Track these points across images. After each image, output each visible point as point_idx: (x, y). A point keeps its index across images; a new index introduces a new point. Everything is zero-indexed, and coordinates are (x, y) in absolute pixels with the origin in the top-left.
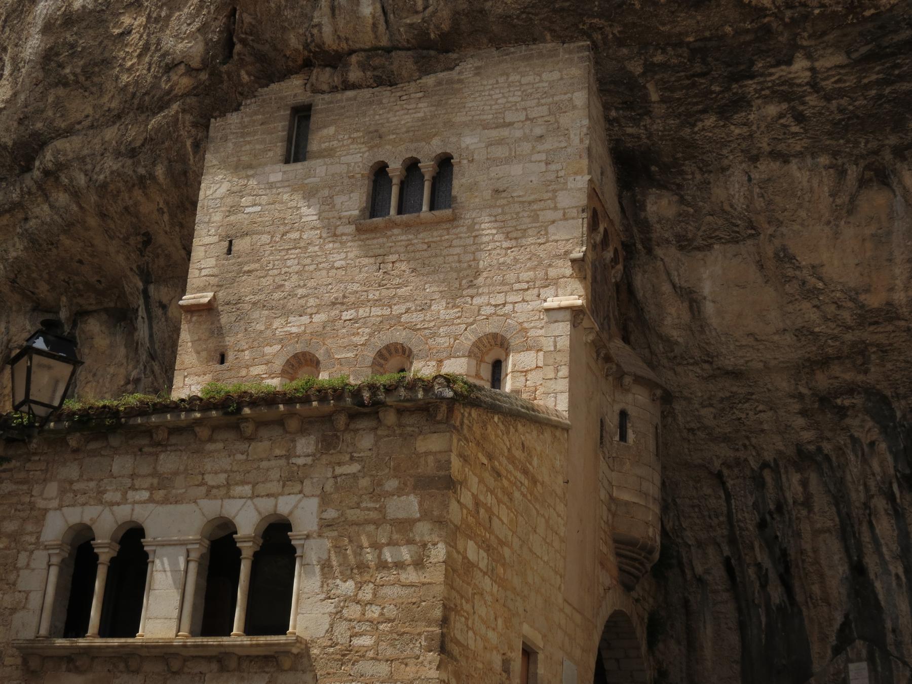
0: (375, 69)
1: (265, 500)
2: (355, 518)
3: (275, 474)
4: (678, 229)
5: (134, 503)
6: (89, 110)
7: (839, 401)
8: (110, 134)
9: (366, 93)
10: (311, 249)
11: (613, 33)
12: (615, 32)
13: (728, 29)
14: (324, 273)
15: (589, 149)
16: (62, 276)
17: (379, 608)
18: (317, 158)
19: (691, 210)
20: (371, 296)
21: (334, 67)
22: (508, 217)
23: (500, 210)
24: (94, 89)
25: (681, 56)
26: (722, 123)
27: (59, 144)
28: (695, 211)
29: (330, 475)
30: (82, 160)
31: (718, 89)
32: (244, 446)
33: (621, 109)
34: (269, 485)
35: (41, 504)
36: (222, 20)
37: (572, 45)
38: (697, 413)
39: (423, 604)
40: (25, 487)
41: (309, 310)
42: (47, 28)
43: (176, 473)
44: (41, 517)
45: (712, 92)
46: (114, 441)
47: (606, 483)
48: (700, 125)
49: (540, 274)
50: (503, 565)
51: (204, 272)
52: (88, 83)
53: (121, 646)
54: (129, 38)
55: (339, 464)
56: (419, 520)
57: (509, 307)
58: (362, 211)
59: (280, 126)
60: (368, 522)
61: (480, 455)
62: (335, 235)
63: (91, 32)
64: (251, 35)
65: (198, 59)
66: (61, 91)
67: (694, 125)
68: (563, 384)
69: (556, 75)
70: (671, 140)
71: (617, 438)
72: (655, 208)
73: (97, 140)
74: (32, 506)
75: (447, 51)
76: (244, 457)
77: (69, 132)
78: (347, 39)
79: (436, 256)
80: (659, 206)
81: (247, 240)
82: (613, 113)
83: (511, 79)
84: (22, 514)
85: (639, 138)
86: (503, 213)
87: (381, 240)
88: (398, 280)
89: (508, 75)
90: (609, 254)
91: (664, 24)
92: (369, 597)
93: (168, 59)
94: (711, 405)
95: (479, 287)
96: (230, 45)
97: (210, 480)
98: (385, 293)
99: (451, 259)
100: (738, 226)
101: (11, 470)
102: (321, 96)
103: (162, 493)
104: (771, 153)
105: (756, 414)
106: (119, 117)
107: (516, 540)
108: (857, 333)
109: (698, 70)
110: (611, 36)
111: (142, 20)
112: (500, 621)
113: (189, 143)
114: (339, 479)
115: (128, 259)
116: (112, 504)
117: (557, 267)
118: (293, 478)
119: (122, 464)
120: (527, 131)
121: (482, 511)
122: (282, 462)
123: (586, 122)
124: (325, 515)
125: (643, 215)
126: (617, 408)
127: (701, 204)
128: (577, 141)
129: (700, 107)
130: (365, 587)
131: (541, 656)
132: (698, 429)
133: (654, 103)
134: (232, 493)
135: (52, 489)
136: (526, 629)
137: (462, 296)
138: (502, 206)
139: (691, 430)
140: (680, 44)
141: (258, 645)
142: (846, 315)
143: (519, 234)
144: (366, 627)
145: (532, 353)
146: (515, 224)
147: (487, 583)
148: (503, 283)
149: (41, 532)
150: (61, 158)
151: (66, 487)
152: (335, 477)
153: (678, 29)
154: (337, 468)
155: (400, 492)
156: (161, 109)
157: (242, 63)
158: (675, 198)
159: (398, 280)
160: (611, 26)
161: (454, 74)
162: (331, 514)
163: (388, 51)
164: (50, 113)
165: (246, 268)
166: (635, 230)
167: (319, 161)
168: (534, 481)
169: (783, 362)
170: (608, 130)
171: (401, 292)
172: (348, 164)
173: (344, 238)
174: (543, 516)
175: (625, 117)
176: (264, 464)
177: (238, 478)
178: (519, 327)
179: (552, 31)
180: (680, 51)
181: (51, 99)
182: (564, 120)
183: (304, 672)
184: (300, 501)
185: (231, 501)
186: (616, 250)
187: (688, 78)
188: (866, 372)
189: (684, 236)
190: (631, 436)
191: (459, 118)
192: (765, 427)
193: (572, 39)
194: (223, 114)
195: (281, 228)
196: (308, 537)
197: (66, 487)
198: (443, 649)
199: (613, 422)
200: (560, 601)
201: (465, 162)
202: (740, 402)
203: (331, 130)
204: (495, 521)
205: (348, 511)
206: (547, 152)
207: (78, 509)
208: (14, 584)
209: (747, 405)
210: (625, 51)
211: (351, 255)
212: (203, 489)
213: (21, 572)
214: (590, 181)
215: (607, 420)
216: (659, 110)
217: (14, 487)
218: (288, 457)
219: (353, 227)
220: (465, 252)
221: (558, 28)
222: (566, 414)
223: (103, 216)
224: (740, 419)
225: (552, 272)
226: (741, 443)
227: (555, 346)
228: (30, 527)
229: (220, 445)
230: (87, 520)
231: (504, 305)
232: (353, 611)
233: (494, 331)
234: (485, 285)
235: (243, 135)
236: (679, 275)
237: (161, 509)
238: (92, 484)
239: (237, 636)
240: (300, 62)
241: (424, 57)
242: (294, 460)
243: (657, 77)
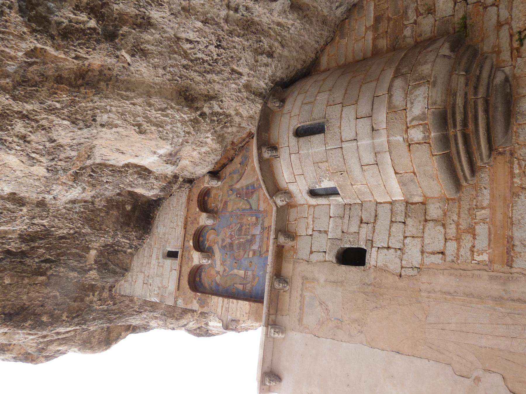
7: (92, 23)
11: (93, 295)
12: (91, 297)
25: (56, 271)
26: (53, 229)
31: (42, 250)
33: (122, 251)
38: (252, 72)
45: (47, 249)
48: (72, 231)
67: (76, 232)
70: (101, 229)
82: (129, 251)
91: (55, 297)
94: (233, 71)
100: (90, 175)
104: (23, 205)
105: (198, 42)
108: (16, 107)
110: (96, 294)
127: (109, 188)
132: (262, 54)
133: (96, 249)
139: (270, 55)
142: (19, 127)
153: (46, 291)
169: (128, 98)
188: (32, 53)
189: (140, 177)
192: (199, 24)
202: (204, 61)
209: (200, 55)
216: (96, 245)
224: (217, 47)
226: (239, 15)
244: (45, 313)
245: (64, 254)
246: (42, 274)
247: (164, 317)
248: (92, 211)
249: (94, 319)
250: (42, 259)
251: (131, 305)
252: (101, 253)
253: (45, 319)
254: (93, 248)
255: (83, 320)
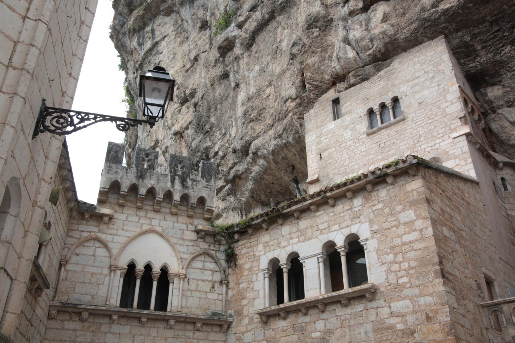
0: (359, 76)
1: (345, 229)
2: (386, 226)
3: (347, 218)
4: (506, 99)
5: (293, 244)
6: (262, 127)
8: (271, 132)
9: (358, 86)
10: (351, 148)
13: (505, 7)
14: (358, 155)
15: (455, 75)
16: (268, 191)
17: (407, 263)
18: (346, 115)
19: (509, 89)
20: (379, 158)
21: (344, 81)
22: (427, 111)
23: (423, 110)
24: (262, 119)
25: (486, 26)
27: (255, 142)
28: (511, 89)
29: (371, 211)
30: (264, 144)
31: (507, 34)
32: (331, 210)
33: (466, 58)
34: (346, 223)
35: (257, 254)
36: (300, 78)
37: (436, 39)
39: (428, 257)
40: (251, 249)
41: (356, 170)
42: (243, 104)
43: (307, 228)
44: (258, 259)
46: (280, 221)
47: (504, 209)
48: (503, 52)
49: (448, 128)
50: (464, 239)
51: (313, 168)
52: (260, 118)
53: (298, 305)
54: (270, 97)
55: (374, 206)
56: (416, 220)
57: (437, 146)
58: (368, 128)
59: (329, 107)
60: (393, 227)
61: (439, 190)
62: (359, 140)
63: (257, 100)
64: (311, 79)
65: (294, 95)
66: (252, 124)
67: (501, 53)
68: (471, 166)
69: (433, 52)
70: (492, 63)
71: (503, 189)
72: (492, 94)
73: (267, 136)
74: (254, 256)
75: (386, 60)
76: (333, 214)
77: (258, 137)
78: (346, 68)
79: (401, 135)
80: (494, 92)
81: (326, 152)
82: (462, 61)
83: (414, 60)
84: (251, 260)
85: (477, 67)
86: (425, 111)
87: (377, 136)
88: (388, 149)
89: (412, 60)
90: (476, 117)
91: (474, 16)
92: (401, 259)
93: (284, 99)
95: (422, 141)
96: (304, 86)
97: (321, 227)
98: (384, 155)
99: (407, 134)
101: (244, 244)
102: (341, 93)
103: (303, 237)
106: (273, 125)
107: (467, 229)
109: (496, 29)
111: (273, 90)
112: (469, 265)
113: (298, 125)
114: (375, 212)
115: (289, 177)
116: (284, 247)
117: (454, 124)
118: (356, 217)
119: (285, 230)
120: (426, 77)
121: (446, 214)
122: (350, 211)
123: (451, 65)
124: (373, 229)
125: (487, 98)
126: (499, 177)
128: (448, 73)
129: (501, 45)
130: (398, 255)
131: (496, 284)
134: (331, 230)
135: (261, 247)
136: (484, 270)
137: (416, 147)
138: (424, 108)
140: (484, 21)
141: (355, 292)
143: (434, 116)
144: (403, 273)
145: (453, 160)
146: (431, 113)
147: (458, 247)
148: (432, 137)
149: (259, 265)
150: (257, 147)
151: (266, 245)
152: (373, 212)
153: (481, 16)
154: (373, 208)
155: (404, 210)
156: (286, 117)
157: (310, 91)
158: (501, 87)
159: (388, 149)
160: (451, 25)
161: (391, 67)
162: (375, 228)
163: (363, 67)
164: (250, 132)
165: (328, 162)
166: (485, 105)
167: (347, 116)
168: (469, 204)
170: (461, 68)
171: (390, 153)
172: (358, 113)
173: (363, 140)
174: (477, 219)
175: (468, 61)
176: (342, 215)
177: (332, 223)
178: (444, 152)
179: (426, 37)
180: (485, 25)
181: (249, 127)
182: (441, 67)
183: (379, 300)
184: (360, 225)
185: (331, 233)
186: (479, 115)
187: (492, 34)
190: (509, 188)
191: (397, 82)
193: (436, 37)
194: (308, 111)
195: (338, 144)
196: (367, 239)
197: (266, 245)
198: (443, 276)
199: (499, 183)
200: (498, 258)
201: (404, 97)
203: (349, 103)
204: (454, 219)
205: (383, 224)
206: (437, 82)
207: (272, 252)
208: (253, 289)
210: (460, 33)
211: (367, 145)
212: (319, 231)
213: (255, 283)
214: (459, 86)
215: (496, 182)
217: (247, 250)
218: (351, 209)
219: (366, 135)
220: (413, 130)
221: (428, 35)
222: (476, 178)
223: (276, 162)
225: (452, 127)
227: (462, 152)
228: (255, 264)
229: (322, 212)
230: (276, 256)
231: (435, 145)
232: (395, 267)
233: (433, 156)
234: (425, 140)
235: (316, 116)
236: (512, 117)
237: (303, 244)
238: (275, 241)
239: (346, 289)
240: (331, 84)
241: (377, 65)
242: (354, 210)
243: (478, 39)
244: (472, 7)
245: (493, 38)
246: (492, 23)
247: (393, 38)
248: (504, 67)
249: (439, 17)
250: (502, 30)
251: (423, 34)
252: (475, 50)
253: (471, 5)
254: (481, 49)
255: (447, 15)
